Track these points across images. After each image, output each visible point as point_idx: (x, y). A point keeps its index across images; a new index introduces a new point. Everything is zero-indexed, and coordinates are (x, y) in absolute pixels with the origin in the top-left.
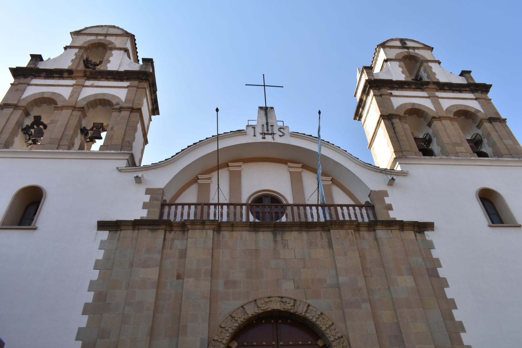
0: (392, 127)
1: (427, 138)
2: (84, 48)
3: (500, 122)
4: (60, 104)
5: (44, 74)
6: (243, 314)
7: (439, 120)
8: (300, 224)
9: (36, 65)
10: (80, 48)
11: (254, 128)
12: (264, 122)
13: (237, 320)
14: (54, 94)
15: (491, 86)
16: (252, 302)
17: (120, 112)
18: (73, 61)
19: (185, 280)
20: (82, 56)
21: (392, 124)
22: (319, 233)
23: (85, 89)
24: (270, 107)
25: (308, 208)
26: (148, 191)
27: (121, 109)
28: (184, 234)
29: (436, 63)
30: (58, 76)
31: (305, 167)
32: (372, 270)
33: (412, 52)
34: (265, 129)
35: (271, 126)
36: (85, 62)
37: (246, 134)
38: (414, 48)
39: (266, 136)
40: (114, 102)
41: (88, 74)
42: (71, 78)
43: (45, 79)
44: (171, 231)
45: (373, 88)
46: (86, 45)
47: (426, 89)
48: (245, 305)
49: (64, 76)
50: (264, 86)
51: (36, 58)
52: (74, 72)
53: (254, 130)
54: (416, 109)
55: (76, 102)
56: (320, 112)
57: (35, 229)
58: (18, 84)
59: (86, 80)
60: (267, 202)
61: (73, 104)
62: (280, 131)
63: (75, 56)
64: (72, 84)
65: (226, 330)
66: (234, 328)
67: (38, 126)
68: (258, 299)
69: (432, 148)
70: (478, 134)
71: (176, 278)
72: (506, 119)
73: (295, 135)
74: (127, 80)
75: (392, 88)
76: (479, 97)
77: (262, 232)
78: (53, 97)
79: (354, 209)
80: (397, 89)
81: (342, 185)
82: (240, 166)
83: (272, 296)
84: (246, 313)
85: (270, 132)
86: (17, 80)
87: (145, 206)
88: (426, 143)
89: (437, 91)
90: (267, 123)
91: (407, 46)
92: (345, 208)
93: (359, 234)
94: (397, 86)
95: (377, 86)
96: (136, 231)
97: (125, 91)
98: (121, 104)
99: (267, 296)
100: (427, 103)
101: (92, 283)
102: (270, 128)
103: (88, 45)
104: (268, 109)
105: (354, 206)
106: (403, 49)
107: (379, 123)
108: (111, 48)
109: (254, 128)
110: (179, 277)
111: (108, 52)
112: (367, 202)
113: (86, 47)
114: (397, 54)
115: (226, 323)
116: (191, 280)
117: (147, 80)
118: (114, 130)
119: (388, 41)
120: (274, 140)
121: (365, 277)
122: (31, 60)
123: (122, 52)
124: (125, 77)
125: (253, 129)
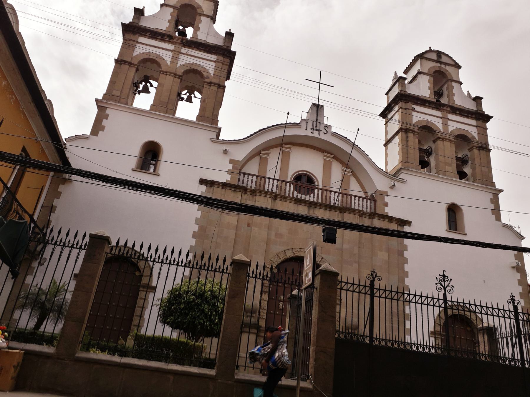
0: (406, 138)
1: (429, 150)
3: (486, 151)
6: (284, 255)
7: (442, 141)
8: (326, 205)
10: (174, 7)
11: (307, 122)
12: (315, 119)
13: (281, 258)
15: (492, 117)
16: (290, 249)
17: (210, 86)
18: (169, 21)
19: (253, 228)
21: (407, 137)
22: (337, 213)
23: (181, 57)
24: (321, 105)
25: (333, 193)
26: (232, 161)
27: (210, 84)
28: (253, 197)
29: (458, 84)
30: (160, 38)
31: (335, 158)
32: (364, 244)
34: (315, 126)
35: (319, 123)
37: (300, 127)
38: (446, 64)
39: (315, 132)
40: (205, 74)
41: (185, 41)
44: (245, 193)
45: (402, 101)
47: (442, 110)
48: (286, 250)
49: (165, 39)
50: (320, 83)
53: (307, 125)
54: (428, 126)
55: (176, 69)
56: (358, 130)
57: (158, 175)
60: (304, 179)
61: (174, 71)
62: (325, 129)
63: (171, 16)
64: (172, 49)
65: (274, 263)
66: (278, 262)
67: (146, 83)
68: (294, 248)
69: (430, 159)
70: (467, 155)
71: (247, 225)
72: (491, 150)
73: (335, 135)
74: (215, 54)
75: (416, 104)
76: (478, 125)
77: (301, 205)
78: (157, 59)
79: (363, 201)
80: (420, 105)
81: (358, 178)
82: (290, 148)
83: (302, 248)
84: (286, 255)
85: (318, 129)
87: (229, 172)
88: (427, 154)
89: (450, 113)
90: (317, 120)
91: (441, 60)
92: (357, 198)
93: (362, 219)
95: (406, 100)
96: (224, 190)
97: (214, 64)
98: (210, 77)
99: (299, 247)
100: (438, 123)
101: (197, 219)
102: (318, 124)
104: (320, 107)
105: (363, 198)
106: (436, 63)
107: (397, 133)
108: (200, 13)
109: (307, 122)
110: (249, 225)
111: (198, 17)
112: (372, 196)
114: (431, 68)
115: (274, 259)
116: (256, 229)
117: (229, 57)
118: (206, 102)
120: (319, 136)
121: (359, 247)
122: (135, 14)
123: (209, 19)
124: (213, 51)
125: (306, 123)
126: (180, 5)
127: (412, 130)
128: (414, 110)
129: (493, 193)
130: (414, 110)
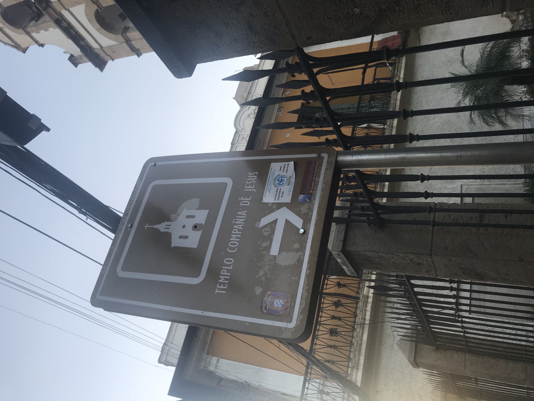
2: (25, 30)
4: (95, 7)
5: (80, 42)
9: (81, 56)
10: (28, 34)
14: (90, 20)
18: (46, 30)
20: (34, 26)
30: (71, 30)
36: (36, 19)
42: (63, 17)
43: (85, 39)
46: (21, 31)
51: (74, 61)
52: (55, 19)
58: (109, 56)
59: (52, 3)
63: (40, 31)
64: (67, 11)
86: (106, 60)
103: (18, 29)
113: (23, 29)
122: (80, 63)
126: (19, 30)
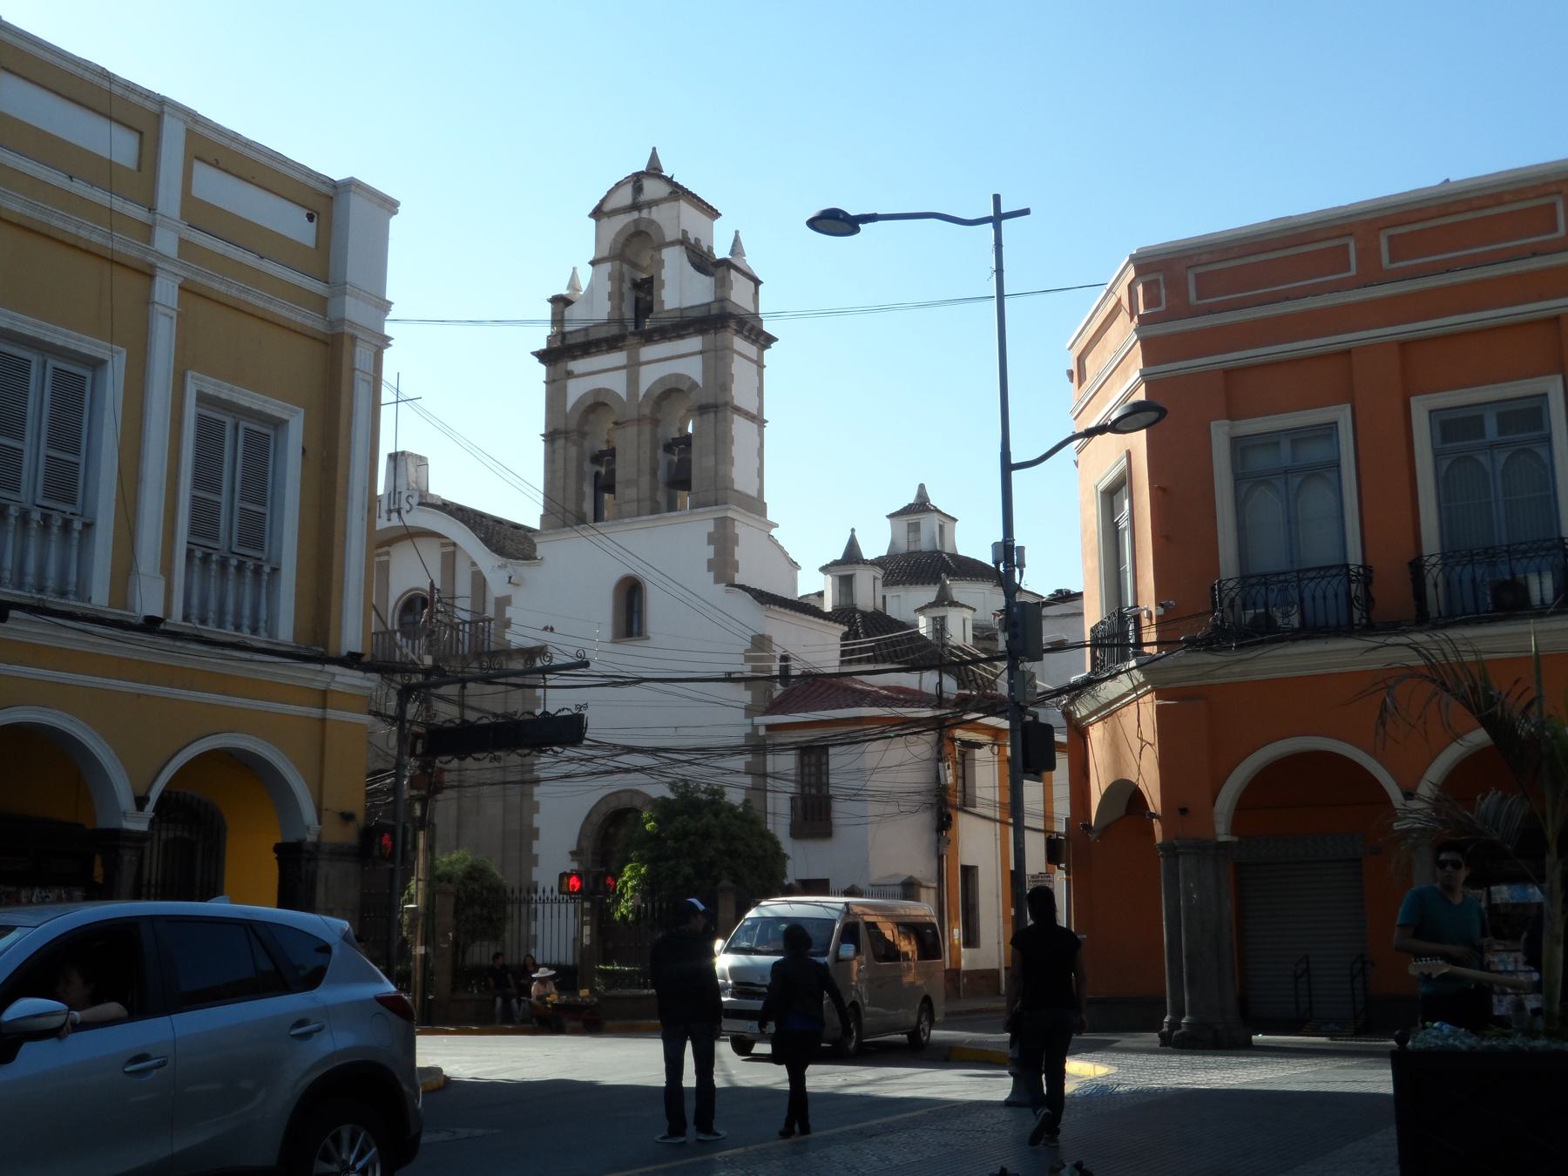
3: (716, 413)
21: (554, 452)
33: (645, 218)
34: (392, 502)
35: (400, 493)
38: (651, 204)
50: (397, 402)
75: (574, 358)
82: (388, 553)
85: (397, 506)
89: (644, 346)
90: (395, 490)
94: (579, 353)
102: (397, 495)
114: (619, 234)
119: (610, 192)
127: (560, 433)
128: (570, 375)
129: (715, 519)
130: (570, 375)
